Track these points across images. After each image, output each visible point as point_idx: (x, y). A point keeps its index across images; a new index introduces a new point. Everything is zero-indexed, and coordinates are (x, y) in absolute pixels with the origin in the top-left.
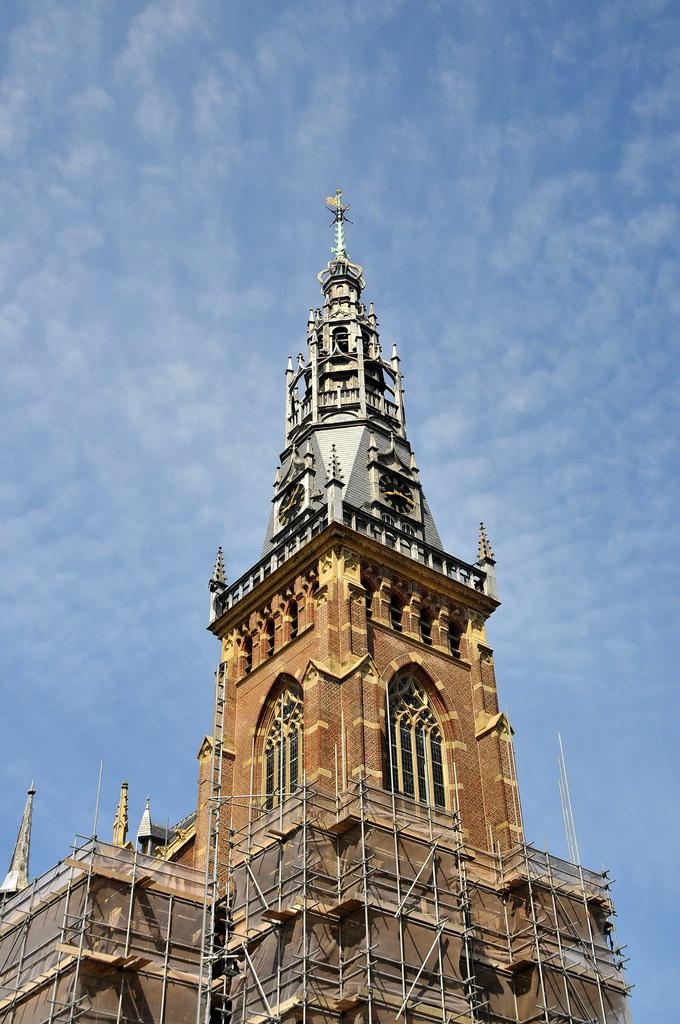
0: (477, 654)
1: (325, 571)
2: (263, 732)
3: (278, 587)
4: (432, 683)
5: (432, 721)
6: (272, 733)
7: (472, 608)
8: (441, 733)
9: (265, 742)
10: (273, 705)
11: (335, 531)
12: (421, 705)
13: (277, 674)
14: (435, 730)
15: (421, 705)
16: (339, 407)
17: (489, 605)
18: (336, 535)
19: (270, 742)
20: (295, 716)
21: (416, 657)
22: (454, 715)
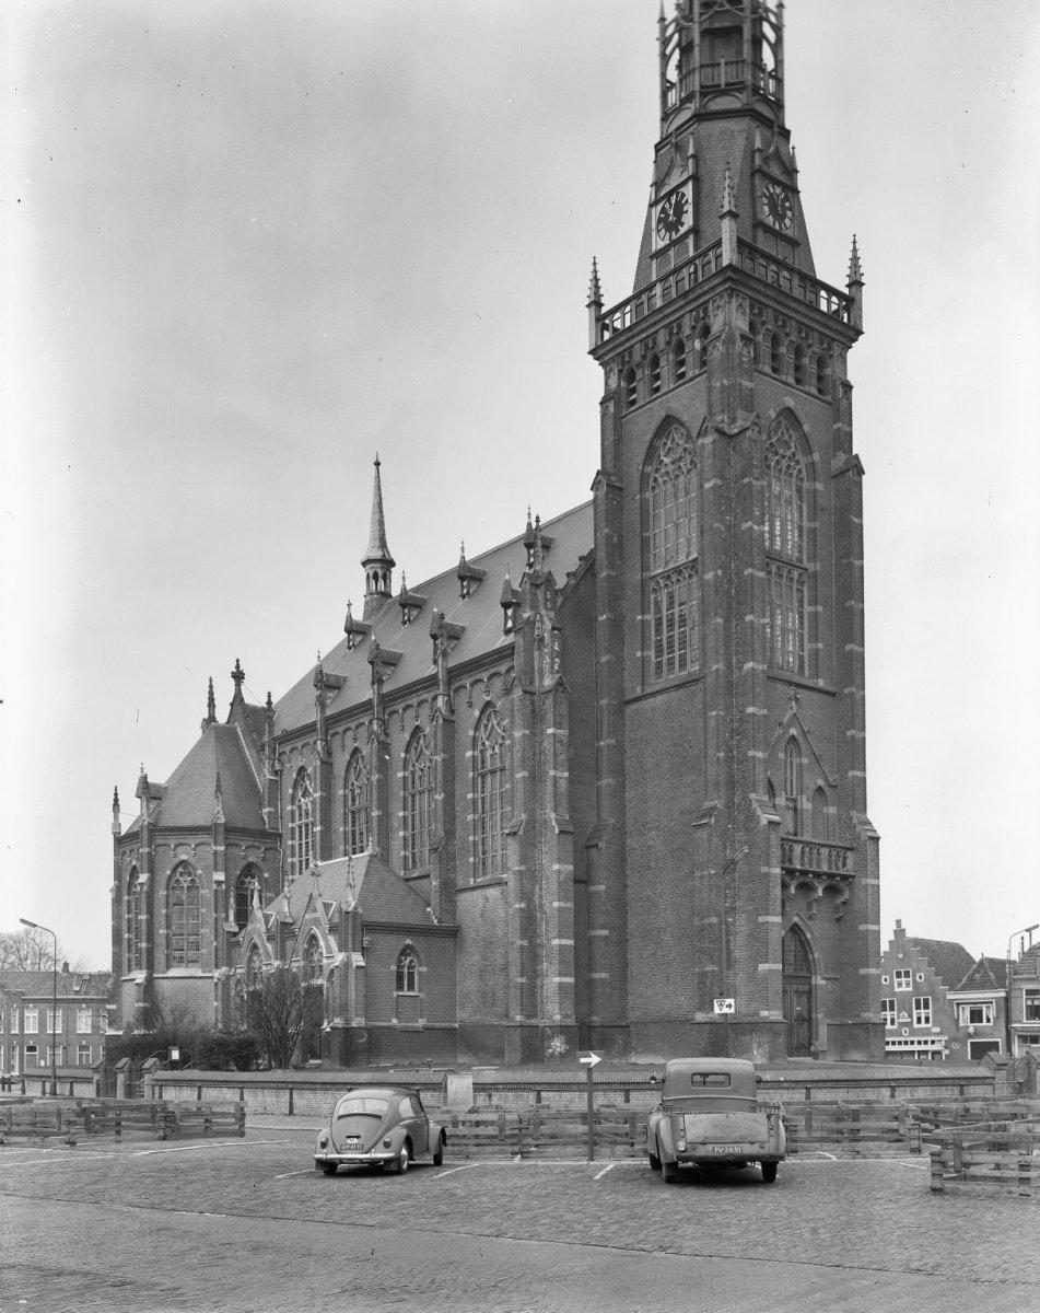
2: (648, 469)
4: (801, 425)
5: (798, 462)
6: (657, 470)
7: (838, 341)
9: (651, 481)
10: (659, 443)
11: (729, 274)
12: (789, 448)
14: (800, 471)
15: (789, 448)
16: (723, 87)
17: (852, 334)
19: (656, 479)
21: (790, 402)
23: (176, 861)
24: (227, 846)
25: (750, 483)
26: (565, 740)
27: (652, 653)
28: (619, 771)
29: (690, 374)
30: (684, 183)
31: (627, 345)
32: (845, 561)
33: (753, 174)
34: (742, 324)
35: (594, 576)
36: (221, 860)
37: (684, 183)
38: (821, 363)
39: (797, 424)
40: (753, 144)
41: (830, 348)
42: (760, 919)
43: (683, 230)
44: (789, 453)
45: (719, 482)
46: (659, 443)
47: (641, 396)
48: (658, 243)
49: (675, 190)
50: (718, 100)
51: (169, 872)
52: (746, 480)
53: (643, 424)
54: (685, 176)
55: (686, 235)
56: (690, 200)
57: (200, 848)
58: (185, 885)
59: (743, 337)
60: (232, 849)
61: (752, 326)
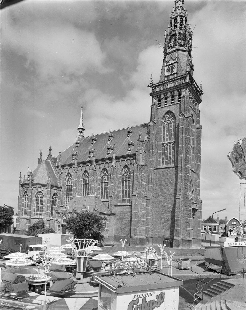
1: (183, 92)
9: (163, 123)
11: (188, 84)
13: (168, 110)
18: (188, 85)
20: (171, 120)
23: (38, 191)
24: (51, 189)
32: (198, 146)
36: (49, 192)
37: (175, 63)
40: (188, 58)
42: (189, 218)
43: (173, 73)
47: (163, 105)
49: (172, 64)
50: (181, 47)
51: (36, 194)
55: (174, 74)
56: (176, 66)
57: (44, 189)
58: (40, 197)
60: (52, 190)
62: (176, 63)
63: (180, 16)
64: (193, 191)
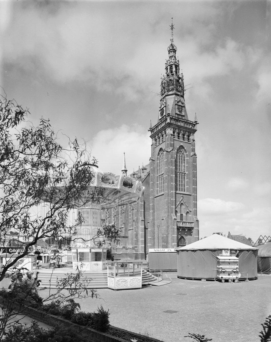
0: (192, 141)
2: (158, 157)
3: (160, 132)
5: (184, 154)
6: (160, 157)
8: (185, 156)
10: (160, 152)
14: (184, 156)
17: (195, 131)
21: (182, 144)
22: (187, 153)
25: (172, 160)
26: (143, 204)
27: (159, 189)
28: (153, 209)
29: (164, 141)
30: (164, 107)
31: (155, 135)
33: (175, 105)
34: (172, 132)
35: (150, 176)
38: (189, 136)
39: (184, 148)
41: (190, 134)
42: (173, 235)
43: (164, 115)
44: (182, 153)
45: (167, 160)
46: (160, 152)
48: (160, 118)
50: (170, 92)
52: (171, 159)
53: (158, 149)
54: (164, 106)
55: (164, 116)
59: (171, 135)
61: (174, 132)
62: (165, 107)
63: (169, 65)
64: (189, 212)
